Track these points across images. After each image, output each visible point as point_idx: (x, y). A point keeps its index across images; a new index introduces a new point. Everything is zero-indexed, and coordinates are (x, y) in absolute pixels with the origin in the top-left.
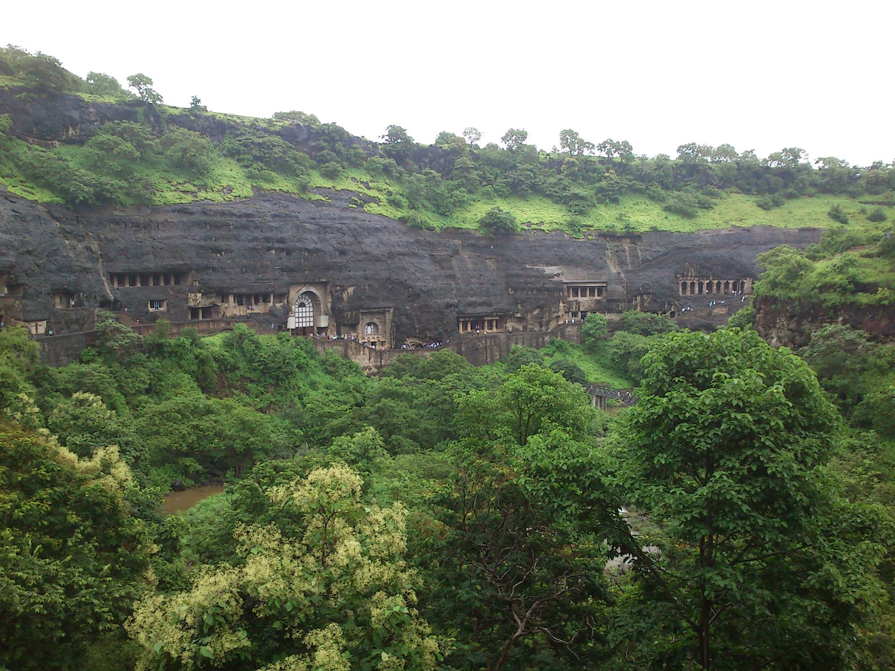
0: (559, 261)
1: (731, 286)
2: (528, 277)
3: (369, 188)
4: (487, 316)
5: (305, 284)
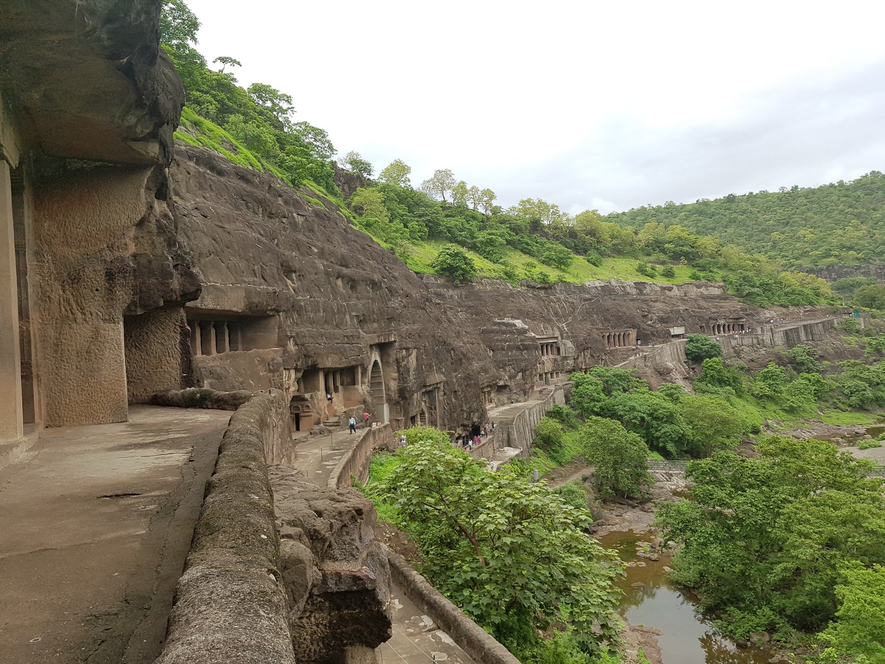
1: (622, 337)
2: (504, 332)
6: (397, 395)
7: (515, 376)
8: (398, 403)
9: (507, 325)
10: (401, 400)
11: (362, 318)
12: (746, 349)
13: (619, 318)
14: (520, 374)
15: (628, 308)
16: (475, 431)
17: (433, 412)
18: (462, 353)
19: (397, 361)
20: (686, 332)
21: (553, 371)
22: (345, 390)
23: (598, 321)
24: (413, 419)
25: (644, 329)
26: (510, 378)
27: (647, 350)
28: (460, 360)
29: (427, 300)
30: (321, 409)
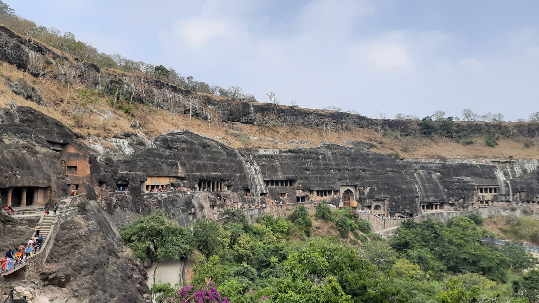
2: (455, 182)
3: (371, 140)
5: (347, 186)
14: (462, 200)
19: (359, 190)
26: (456, 201)
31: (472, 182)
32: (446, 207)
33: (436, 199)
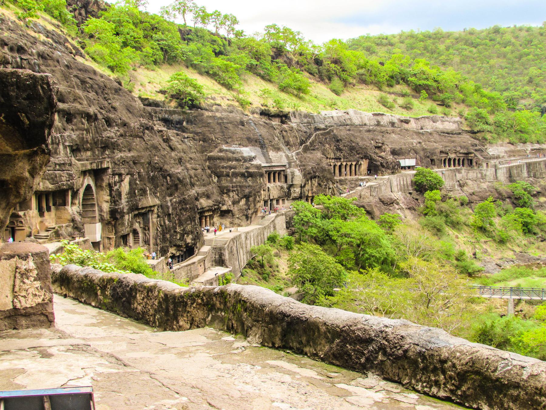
0: (252, 141)
1: (353, 167)
2: (229, 160)
4: (208, 211)
6: (108, 216)
7: (239, 202)
8: (109, 223)
9: (233, 153)
10: (114, 219)
11: (74, 148)
12: (470, 182)
13: (352, 149)
14: (243, 202)
15: (362, 139)
16: (190, 251)
17: (146, 232)
18: (179, 179)
19: (110, 186)
20: (417, 164)
21: (279, 198)
22: (57, 209)
23: (330, 151)
24: (125, 238)
25: (376, 161)
26: (234, 203)
27: (374, 181)
28: (176, 185)
29: (147, 129)
30: (32, 225)
31: (254, 158)
32: (216, 219)
33: (210, 202)
